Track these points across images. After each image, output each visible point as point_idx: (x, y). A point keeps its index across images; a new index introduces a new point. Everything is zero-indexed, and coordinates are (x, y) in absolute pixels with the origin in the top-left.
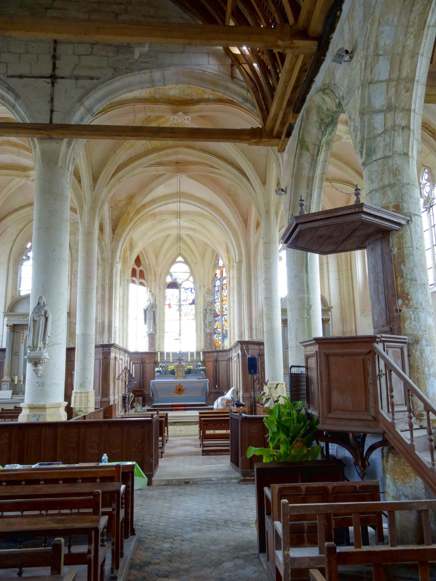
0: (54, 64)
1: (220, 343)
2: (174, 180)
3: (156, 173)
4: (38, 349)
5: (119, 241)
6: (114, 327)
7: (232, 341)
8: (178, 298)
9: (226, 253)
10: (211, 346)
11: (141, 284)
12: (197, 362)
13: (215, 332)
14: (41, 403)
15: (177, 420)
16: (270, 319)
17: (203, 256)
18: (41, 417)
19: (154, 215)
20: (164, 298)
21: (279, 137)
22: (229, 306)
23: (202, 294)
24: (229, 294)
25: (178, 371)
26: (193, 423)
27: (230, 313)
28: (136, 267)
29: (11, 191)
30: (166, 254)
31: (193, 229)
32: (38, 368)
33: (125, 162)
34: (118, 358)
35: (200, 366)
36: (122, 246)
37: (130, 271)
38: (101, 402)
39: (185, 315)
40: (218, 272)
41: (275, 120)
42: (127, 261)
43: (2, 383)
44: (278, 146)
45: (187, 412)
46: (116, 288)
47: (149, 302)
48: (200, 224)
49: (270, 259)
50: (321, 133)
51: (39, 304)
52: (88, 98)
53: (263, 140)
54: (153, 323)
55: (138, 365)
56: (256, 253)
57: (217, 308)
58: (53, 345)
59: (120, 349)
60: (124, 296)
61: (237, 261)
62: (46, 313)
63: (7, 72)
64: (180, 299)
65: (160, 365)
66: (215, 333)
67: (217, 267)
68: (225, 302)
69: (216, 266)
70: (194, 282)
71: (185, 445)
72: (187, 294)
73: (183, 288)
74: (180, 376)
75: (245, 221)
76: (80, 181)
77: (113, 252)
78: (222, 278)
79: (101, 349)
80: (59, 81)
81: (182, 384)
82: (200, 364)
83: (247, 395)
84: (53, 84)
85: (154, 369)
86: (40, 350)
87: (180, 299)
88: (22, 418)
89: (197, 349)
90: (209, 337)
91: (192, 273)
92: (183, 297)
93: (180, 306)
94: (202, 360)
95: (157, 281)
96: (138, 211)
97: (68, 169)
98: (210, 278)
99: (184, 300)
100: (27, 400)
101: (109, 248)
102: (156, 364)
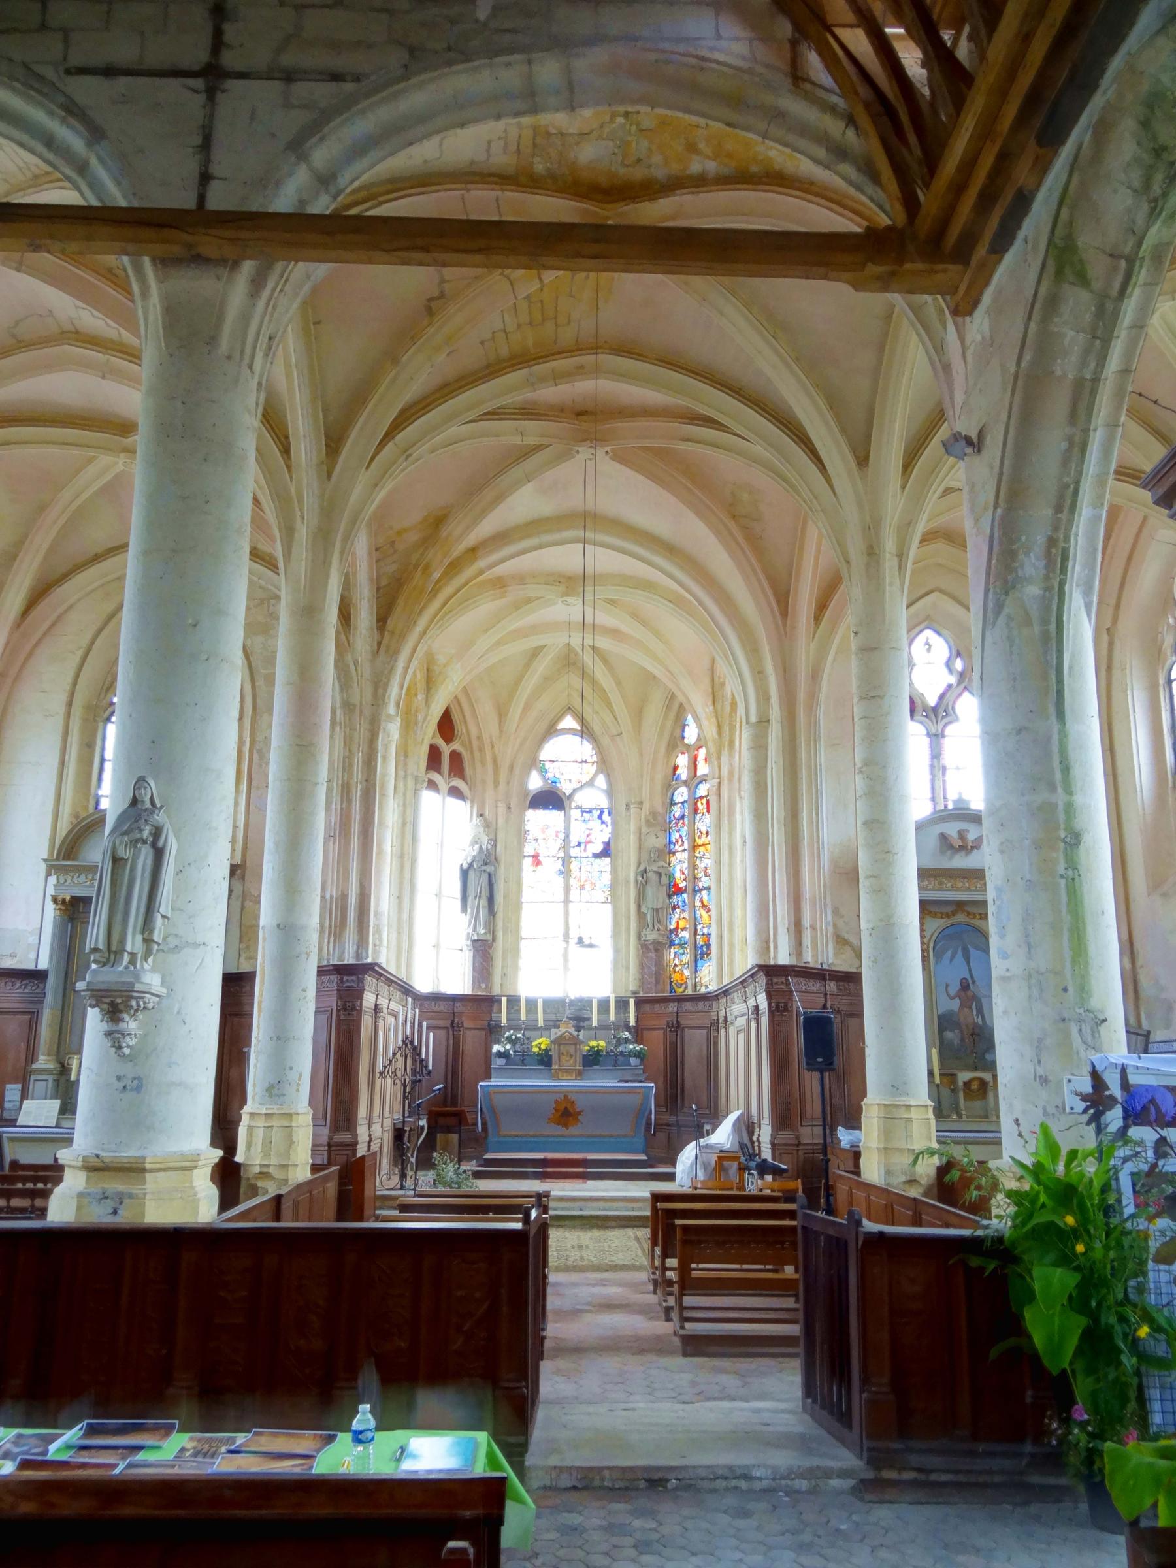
0: (218, 34)
1: (687, 973)
2: (571, 469)
3: (517, 440)
4: (126, 957)
5: (397, 652)
6: (376, 914)
7: (726, 969)
8: (562, 836)
9: (710, 702)
10: (657, 982)
11: (455, 792)
12: (617, 1028)
13: (669, 939)
14: (129, 1153)
15: (563, 1209)
16: (884, 891)
17: (638, 714)
18: (127, 1201)
19: (500, 584)
20: (521, 835)
21: (962, 254)
22: (718, 863)
23: (633, 827)
24: (718, 827)
25: (560, 1054)
26: (614, 1224)
27: (719, 880)
28: (440, 742)
29: (85, 496)
30: (527, 707)
31: (614, 633)
32: (122, 1026)
33: (425, 398)
34: (385, 1011)
35: (627, 1041)
36: (406, 669)
37: (425, 750)
38: (329, 1145)
39: (582, 887)
40: (682, 761)
41: (958, 188)
42: (416, 723)
43: (32, 1078)
44: (954, 291)
45: (591, 1183)
46: (383, 795)
47: (477, 847)
48: (635, 615)
49: (881, 697)
50: (1145, 207)
51: (135, 802)
52: (322, 139)
53: (908, 266)
54: (486, 910)
55: (442, 1034)
56: (813, 696)
57: (678, 868)
58: (177, 949)
59: (390, 982)
60: (404, 824)
61: (753, 719)
62: (157, 832)
63: (65, 59)
64: (566, 840)
65: (507, 1034)
66: (672, 944)
67: (681, 748)
68: (702, 849)
69: (676, 742)
70: (610, 793)
71: (608, 1306)
72: (590, 825)
73: (577, 807)
74: (568, 1071)
75: (782, 598)
76: (286, 451)
77: (380, 685)
78: (694, 780)
79: (335, 978)
80: (232, 84)
81: (572, 1097)
82: (626, 1034)
83: (787, 1137)
84: (211, 93)
85: (488, 1049)
86: (133, 962)
87: (566, 840)
88: (63, 1208)
89: (614, 991)
90: (653, 955)
91: (604, 764)
92: (576, 835)
93: (566, 860)
94: (633, 1023)
95: (502, 786)
96: (454, 567)
97: (250, 367)
98: (659, 777)
99: (579, 845)
100: (85, 1139)
101: (367, 671)
102: (493, 1031)
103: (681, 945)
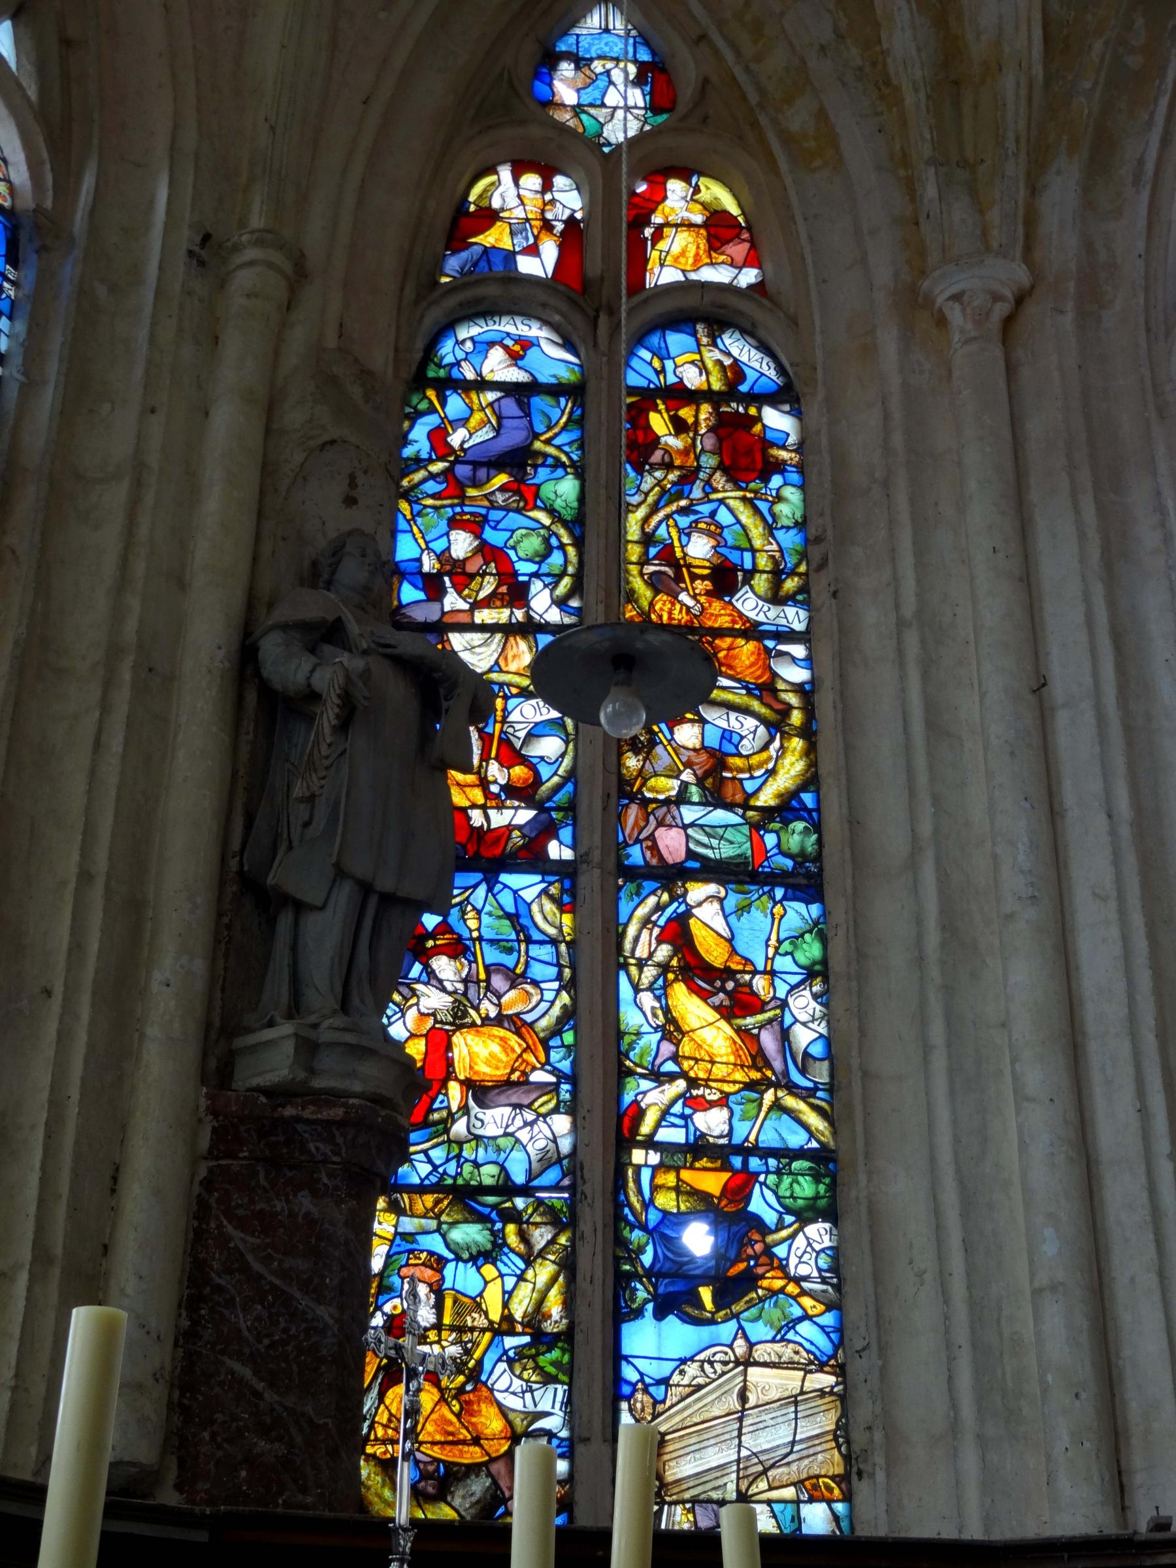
103: (463, 1197)
